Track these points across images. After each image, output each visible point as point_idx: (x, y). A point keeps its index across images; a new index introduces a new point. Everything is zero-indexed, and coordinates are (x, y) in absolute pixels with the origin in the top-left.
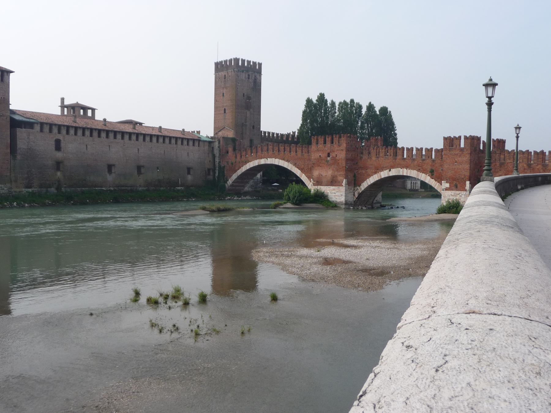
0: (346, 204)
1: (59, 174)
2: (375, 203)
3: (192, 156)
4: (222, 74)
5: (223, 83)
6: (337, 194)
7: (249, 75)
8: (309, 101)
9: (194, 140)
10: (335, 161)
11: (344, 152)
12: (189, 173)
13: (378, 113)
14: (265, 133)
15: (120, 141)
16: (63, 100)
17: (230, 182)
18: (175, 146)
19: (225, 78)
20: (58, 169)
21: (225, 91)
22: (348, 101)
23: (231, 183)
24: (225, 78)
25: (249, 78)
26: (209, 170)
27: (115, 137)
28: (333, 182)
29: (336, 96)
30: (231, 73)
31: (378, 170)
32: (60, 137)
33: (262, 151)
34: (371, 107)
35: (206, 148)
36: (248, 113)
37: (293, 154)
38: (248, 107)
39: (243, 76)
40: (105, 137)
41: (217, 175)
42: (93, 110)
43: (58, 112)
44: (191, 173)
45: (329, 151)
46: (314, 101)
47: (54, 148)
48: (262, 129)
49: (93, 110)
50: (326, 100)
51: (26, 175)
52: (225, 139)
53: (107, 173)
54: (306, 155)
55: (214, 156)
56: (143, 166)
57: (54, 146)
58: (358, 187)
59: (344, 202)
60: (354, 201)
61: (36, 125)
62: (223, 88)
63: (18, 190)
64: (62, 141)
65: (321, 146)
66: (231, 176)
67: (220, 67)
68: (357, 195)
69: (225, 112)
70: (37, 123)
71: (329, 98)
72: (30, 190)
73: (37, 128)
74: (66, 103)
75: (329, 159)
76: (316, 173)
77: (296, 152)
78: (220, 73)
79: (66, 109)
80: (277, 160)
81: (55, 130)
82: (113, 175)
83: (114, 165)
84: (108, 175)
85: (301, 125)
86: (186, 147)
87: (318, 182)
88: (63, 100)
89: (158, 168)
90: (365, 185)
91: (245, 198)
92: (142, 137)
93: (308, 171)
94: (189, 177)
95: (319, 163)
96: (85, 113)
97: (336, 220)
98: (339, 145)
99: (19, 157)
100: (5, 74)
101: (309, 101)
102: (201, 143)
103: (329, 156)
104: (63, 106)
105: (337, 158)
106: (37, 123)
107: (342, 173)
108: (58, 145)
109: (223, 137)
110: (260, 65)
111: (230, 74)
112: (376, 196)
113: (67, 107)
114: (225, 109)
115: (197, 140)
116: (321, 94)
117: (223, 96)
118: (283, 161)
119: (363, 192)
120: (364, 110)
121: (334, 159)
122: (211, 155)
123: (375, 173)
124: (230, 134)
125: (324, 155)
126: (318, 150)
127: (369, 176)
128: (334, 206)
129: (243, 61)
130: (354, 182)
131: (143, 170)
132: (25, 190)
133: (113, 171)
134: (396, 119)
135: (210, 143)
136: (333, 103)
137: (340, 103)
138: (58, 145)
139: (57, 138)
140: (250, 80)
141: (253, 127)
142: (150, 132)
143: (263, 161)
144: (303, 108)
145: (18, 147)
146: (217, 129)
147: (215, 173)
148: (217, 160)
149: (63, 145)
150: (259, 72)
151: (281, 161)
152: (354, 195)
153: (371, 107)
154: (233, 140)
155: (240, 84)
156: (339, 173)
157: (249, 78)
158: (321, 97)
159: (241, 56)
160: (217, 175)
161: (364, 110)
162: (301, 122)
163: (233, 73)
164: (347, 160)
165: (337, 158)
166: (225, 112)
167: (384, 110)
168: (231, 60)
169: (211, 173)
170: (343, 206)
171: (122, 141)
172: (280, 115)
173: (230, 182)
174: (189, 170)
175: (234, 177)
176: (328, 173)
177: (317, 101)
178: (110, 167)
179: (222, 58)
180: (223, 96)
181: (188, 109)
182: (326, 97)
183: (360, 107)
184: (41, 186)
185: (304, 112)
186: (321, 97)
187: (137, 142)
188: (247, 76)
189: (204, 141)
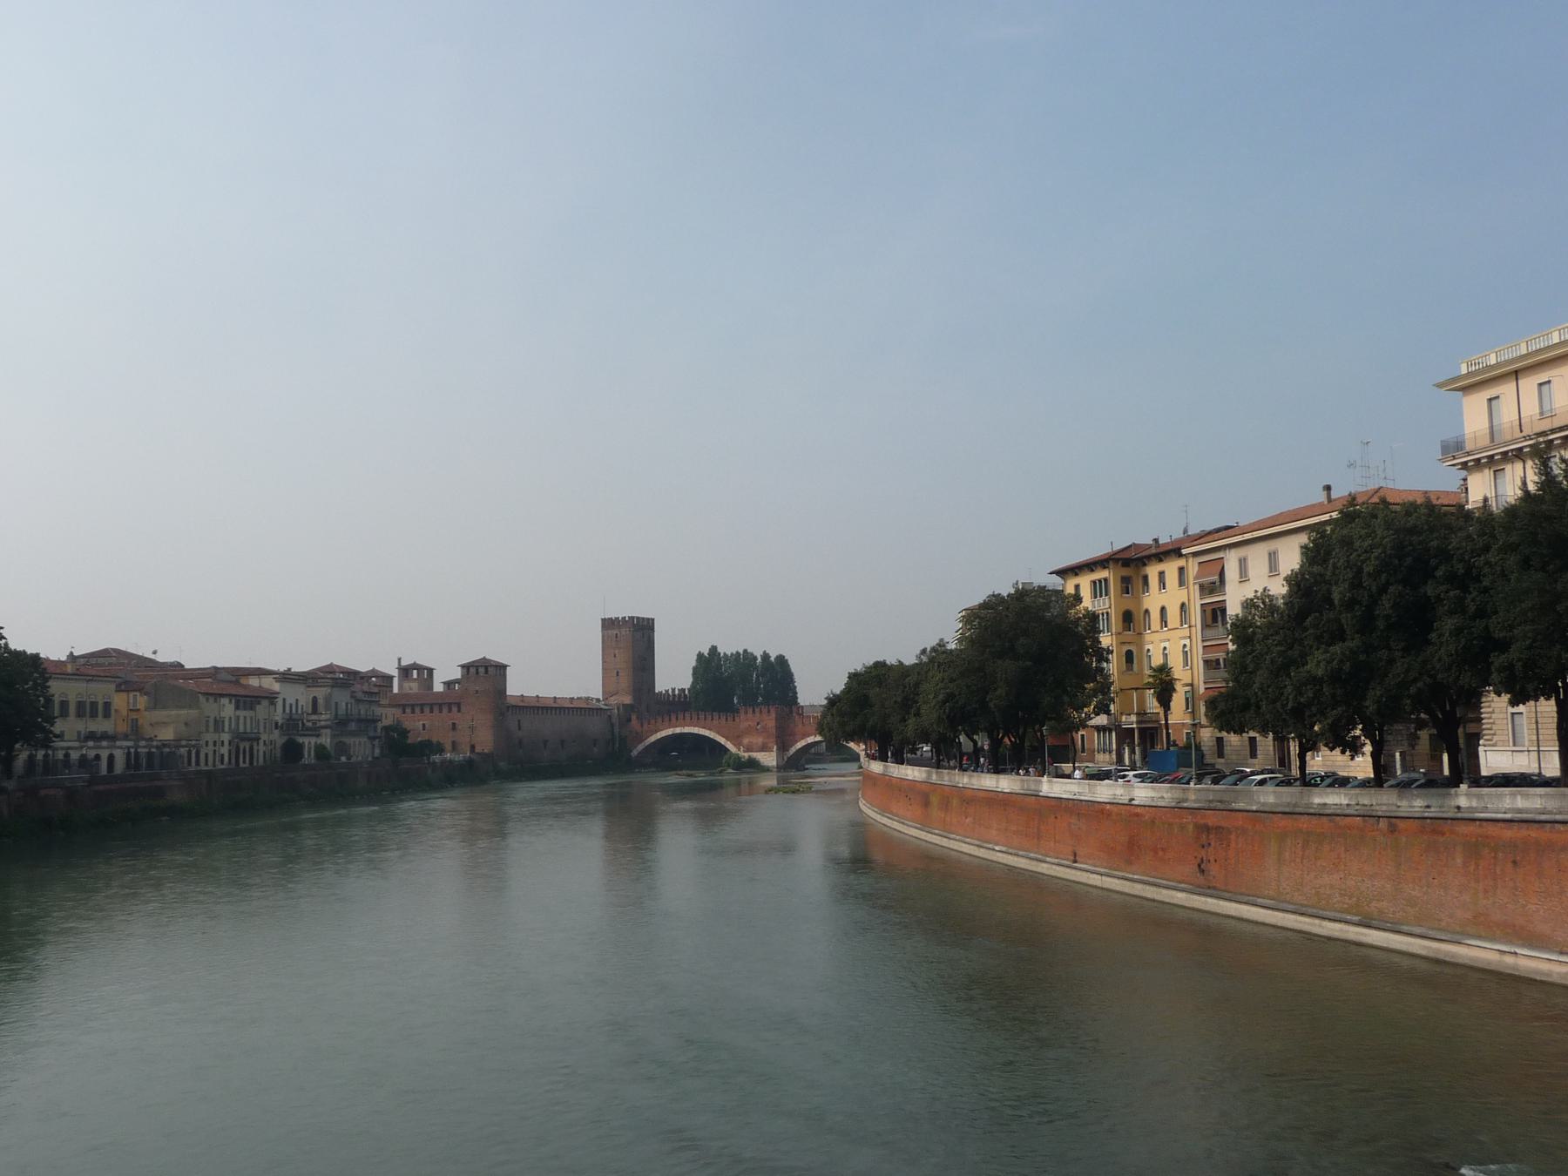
6: (769, 759)
8: (700, 656)
17: (635, 753)
28: (764, 748)
29: (726, 649)
30: (625, 632)
31: (805, 736)
34: (766, 656)
54: (730, 722)
55: (612, 725)
65: (750, 715)
67: (608, 624)
71: (721, 650)
74: (404, 663)
76: (746, 741)
87: (748, 750)
90: (793, 750)
93: (737, 741)
95: (748, 731)
97: (770, 781)
101: (700, 656)
121: (764, 728)
124: (628, 700)
128: (767, 769)
130: (783, 747)
134: (793, 668)
143: (678, 730)
146: (607, 693)
148: (617, 730)
150: (652, 629)
154: (631, 706)
155: (632, 640)
158: (714, 649)
164: (777, 728)
167: (781, 660)
173: (635, 753)
175: (640, 747)
176: (759, 740)
179: (613, 614)
181: (559, 667)
185: (695, 669)
186: (714, 649)
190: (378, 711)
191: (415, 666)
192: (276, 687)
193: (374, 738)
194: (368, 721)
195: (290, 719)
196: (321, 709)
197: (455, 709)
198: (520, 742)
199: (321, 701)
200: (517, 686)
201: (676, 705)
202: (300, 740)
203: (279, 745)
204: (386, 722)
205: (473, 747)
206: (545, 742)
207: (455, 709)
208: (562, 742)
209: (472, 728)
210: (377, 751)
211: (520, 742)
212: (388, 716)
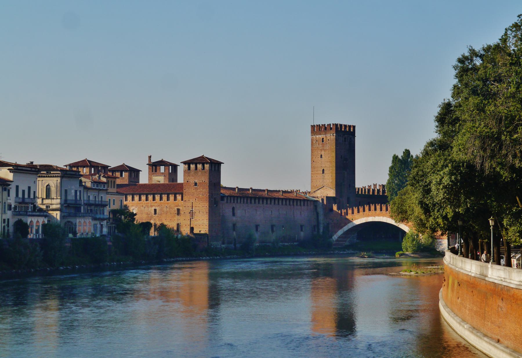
1: (234, 233)
3: (302, 215)
7: (345, 138)
8: (395, 158)
9: (304, 200)
12: (302, 230)
16: (150, 157)
17: (335, 237)
18: (292, 206)
19: (323, 141)
21: (323, 153)
23: (336, 238)
24: (323, 141)
26: (314, 226)
30: (331, 137)
32: (234, 205)
35: (312, 206)
41: (321, 231)
44: (303, 229)
46: (400, 157)
48: (357, 186)
50: (412, 156)
55: (317, 214)
62: (321, 150)
66: (336, 232)
74: (153, 160)
78: (317, 136)
82: (259, 233)
85: (389, 180)
86: (299, 207)
89: (283, 227)
94: (302, 234)
101: (395, 158)
109: (327, 197)
110: (354, 127)
114: (323, 170)
124: (332, 193)
131: (274, 229)
133: (259, 230)
143: (370, 219)
144: (390, 164)
147: (319, 229)
148: (321, 218)
150: (353, 134)
157: (345, 141)
158: (407, 153)
159: (339, 122)
160: (321, 231)
163: (332, 137)
169: (316, 230)
172: (371, 172)
173: (335, 237)
175: (340, 232)
177: (402, 157)
180: (321, 156)
182: (411, 153)
186: (407, 153)
188: (344, 139)
190: (106, 198)
191: (162, 163)
192: (10, 176)
193: (103, 219)
194: (96, 205)
195: (23, 202)
196: (53, 195)
197: (179, 197)
198: (234, 225)
199: (53, 189)
201: (373, 198)
202: (28, 220)
203: (11, 223)
204: (116, 206)
205: (192, 229)
206: (257, 227)
207: (179, 197)
208: (272, 227)
209: (192, 213)
210: (105, 230)
211: (234, 225)
212: (114, 202)
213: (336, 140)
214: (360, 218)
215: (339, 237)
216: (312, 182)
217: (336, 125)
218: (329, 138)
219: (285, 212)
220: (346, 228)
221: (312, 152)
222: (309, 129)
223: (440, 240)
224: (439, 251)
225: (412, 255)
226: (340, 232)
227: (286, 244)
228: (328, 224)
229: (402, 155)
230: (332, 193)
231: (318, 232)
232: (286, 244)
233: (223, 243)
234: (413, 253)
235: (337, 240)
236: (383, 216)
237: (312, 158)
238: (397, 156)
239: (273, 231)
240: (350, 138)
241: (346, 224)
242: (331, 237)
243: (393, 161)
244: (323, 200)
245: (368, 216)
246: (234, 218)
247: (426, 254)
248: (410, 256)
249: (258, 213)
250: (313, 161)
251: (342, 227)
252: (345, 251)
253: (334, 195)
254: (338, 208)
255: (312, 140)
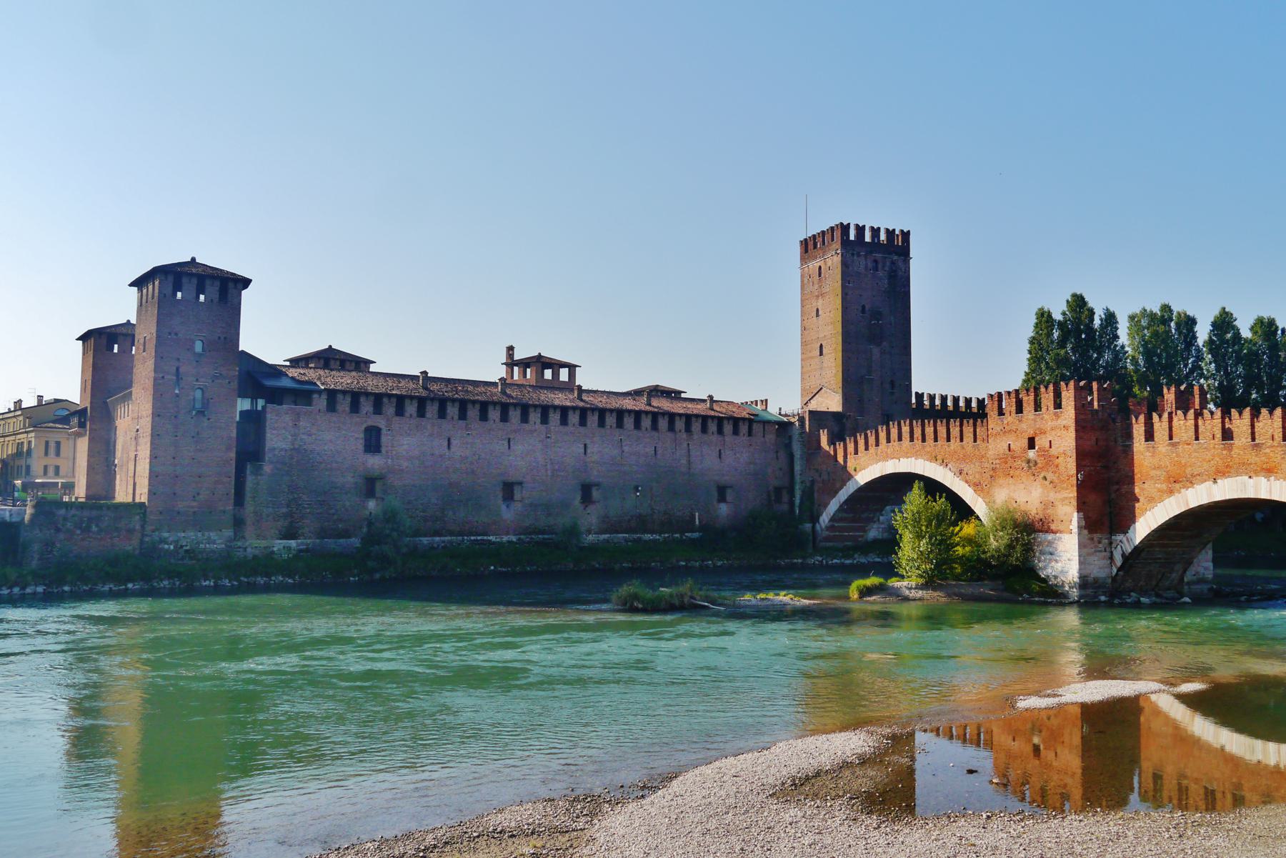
0: (1084, 582)
1: (372, 504)
2: (1188, 583)
4: (814, 265)
5: (816, 286)
7: (876, 261)
8: (1044, 318)
10: (1050, 460)
11: (1072, 434)
12: (722, 499)
13: (1246, 333)
14: (920, 396)
15: (539, 426)
16: (510, 349)
18: (684, 436)
20: (370, 493)
21: (820, 301)
22: (1156, 310)
25: (876, 269)
26: (778, 490)
27: (525, 419)
30: (832, 260)
31: (1178, 480)
32: (380, 422)
33: (888, 440)
34: (1224, 323)
35: (771, 437)
36: (876, 351)
37: (955, 443)
38: (876, 337)
39: (861, 264)
40: (498, 420)
41: (797, 501)
42: (572, 368)
43: (502, 372)
44: (729, 498)
45: (1031, 433)
46: (1057, 316)
47: (361, 447)
48: (916, 387)
49: (572, 368)
50: (1092, 312)
51: (284, 510)
52: (819, 418)
53: (500, 501)
55: (791, 457)
56: (598, 485)
57: (362, 441)
58: (1120, 537)
59: (1076, 580)
60: (1114, 579)
61: (315, 396)
63: (263, 543)
64: (384, 431)
66: (826, 506)
68: (1118, 560)
69: (821, 354)
70: (432, 400)
71: (1098, 307)
72: (293, 543)
73: (321, 402)
74: (518, 356)
75: (1031, 454)
77: (962, 440)
79: (516, 369)
80: (920, 461)
81: (367, 406)
82: (517, 506)
83: (520, 483)
84: (504, 507)
88: (510, 349)
89: (636, 489)
91: (863, 560)
92: (596, 417)
94: (724, 509)
95: (1005, 467)
96: (556, 375)
98: (1056, 414)
99: (267, 468)
100: (231, 285)
101: (1044, 318)
102: (755, 426)
103: (1031, 443)
104: (511, 363)
105: (1053, 451)
106: (432, 400)
107: (1065, 494)
108: (373, 442)
109: (810, 412)
110: (906, 235)
111: (829, 263)
112: (1189, 563)
113: (525, 364)
115: (744, 419)
116: (1074, 295)
117: (817, 315)
118: (933, 465)
119: (1136, 548)
120: (1203, 332)
121: (1045, 453)
122: (782, 454)
123: (1171, 492)
124: (832, 402)
125: (1020, 444)
126: (1005, 432)
127: (1152, 501)
129: (860, 230)
131: (595, 494)
132: (278, 545)
133: (517, 496)
135: (783, 427)
136: (1110, 318)
137: (1132, 318)
138: (373, 442)
139: (370, 423)
140: (880, 273)
141: (892, 384)
142: (601, 402)
144: (1029, 332)
145: (269, 445)
148: (797, 468)
149: (384, 440)
150: (904, 252)
151: (928, 463)
152: (1111, 558)
153: (1224, 323)
156: (1059, 496)
158: (1078, 303)
159: (853, 220)
160: (797, 501)
161: (1203, 332)
162: (1025, 367)
164: (1082, 456)
165: (1053, 451)
166: (821, 354)
168: (832, 228)
169: (785, 498)
170: (1075, 594)
171: (543, 427)
173: (825, 519)
174: (722, 492)
175: (833, 506)
177: (1064, 314)
178: (509, 490)
180: (817, 315)
182: (1092, 302)
183: (1190, 322)
184: (322, 534)
186: (1078, 303)
187: (582, 429)
188: (870, 265)
189: (766, 423)
200: (272, 332)
213: (845, 264)
214: (868, 468)
215: (832, 519)
216: (803, 379)
217: (845, 228)
218: (829, 263)
219: (650, 450)
220: (843, 495)
221: (802, 306)
222: (797, 250)
223: (1050, 537)
224: (1045, 581)
225: (920, 593)
226: (833, 506)
227: (648, 537)
228: (813, 482)
229: (1064, 307)
230: (832, 402)
231: (792, 503)
232: (648, 537)
233: (290, 534)
234: (924, 587)
235: (830, 528)
236: (917, 455)
237: (803, 320)
238: (1049, 315)
239: (587, 498)
240: (893, 263)
241: (844, 483)
242: (815, 519)
243: (1036, 326)
244: (802, 420)
245: (887, 457)
246: (375, 462)
247: (985, 589)
248: (906, 599)
249: (518, 448)
250: (804, 329)
251: (836, 492)
252: (847, 557)
253: (839, 409)
254: (832, 442)
255: (802, 276)
